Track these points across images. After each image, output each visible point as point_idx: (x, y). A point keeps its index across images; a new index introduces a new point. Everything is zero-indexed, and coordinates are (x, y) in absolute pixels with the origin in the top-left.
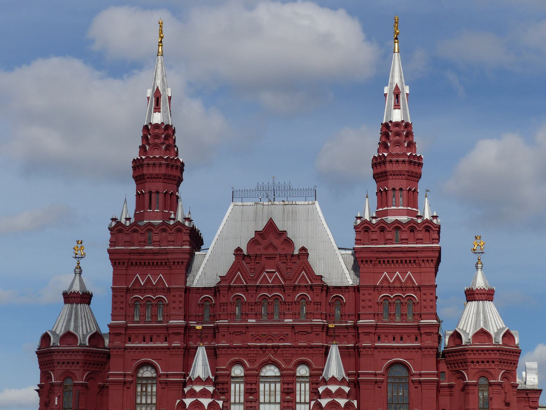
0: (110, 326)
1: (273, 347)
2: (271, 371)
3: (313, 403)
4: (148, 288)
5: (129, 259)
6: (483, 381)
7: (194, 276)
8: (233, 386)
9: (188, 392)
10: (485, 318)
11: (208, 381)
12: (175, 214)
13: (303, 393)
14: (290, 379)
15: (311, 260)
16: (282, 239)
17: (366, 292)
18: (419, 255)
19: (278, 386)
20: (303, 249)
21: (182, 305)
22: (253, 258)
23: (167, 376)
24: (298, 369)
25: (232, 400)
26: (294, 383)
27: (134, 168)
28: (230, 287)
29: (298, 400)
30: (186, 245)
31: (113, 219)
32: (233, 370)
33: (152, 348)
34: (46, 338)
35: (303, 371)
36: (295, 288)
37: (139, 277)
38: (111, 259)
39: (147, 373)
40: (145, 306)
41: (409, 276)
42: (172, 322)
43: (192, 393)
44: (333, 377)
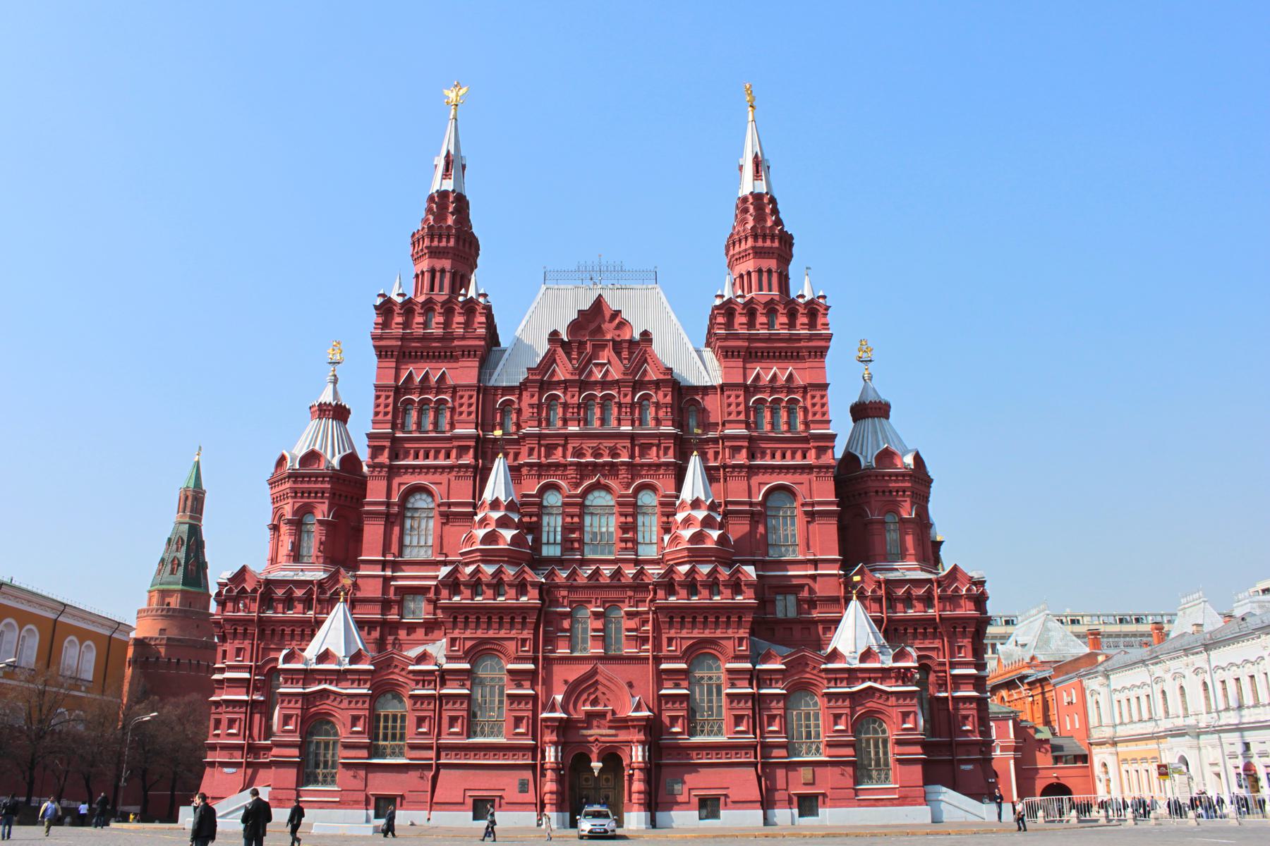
0: (370, 436)
1: (606, 464)
2: (599, 499)
3: (667, 538)
4: (424, 386)
5: (401, 347)
6: (888, 518)
7: (491, 375)
10: (886, 439)
11: (511, 506)
12: (467, 291)
14: (630, 510)
15: (656, 347)
16: (617, 321)
17: (733, 393)
18: (802, 344)
20: (646, 335)
21: (473, 408)
22: (575, 345)
23: (449, 505)
24: (640, 496)
25: (544, 540)
26: (634, 516)
31: (383, 295)
34: (282, 460)
35: (647, 499)
36: (637, 386)
38: (375, 347)
39: (420, 501)
40: (421, 412)
41: (791, 374)
42: (457, 431)
43: (484, 522)
44: (697, 499)
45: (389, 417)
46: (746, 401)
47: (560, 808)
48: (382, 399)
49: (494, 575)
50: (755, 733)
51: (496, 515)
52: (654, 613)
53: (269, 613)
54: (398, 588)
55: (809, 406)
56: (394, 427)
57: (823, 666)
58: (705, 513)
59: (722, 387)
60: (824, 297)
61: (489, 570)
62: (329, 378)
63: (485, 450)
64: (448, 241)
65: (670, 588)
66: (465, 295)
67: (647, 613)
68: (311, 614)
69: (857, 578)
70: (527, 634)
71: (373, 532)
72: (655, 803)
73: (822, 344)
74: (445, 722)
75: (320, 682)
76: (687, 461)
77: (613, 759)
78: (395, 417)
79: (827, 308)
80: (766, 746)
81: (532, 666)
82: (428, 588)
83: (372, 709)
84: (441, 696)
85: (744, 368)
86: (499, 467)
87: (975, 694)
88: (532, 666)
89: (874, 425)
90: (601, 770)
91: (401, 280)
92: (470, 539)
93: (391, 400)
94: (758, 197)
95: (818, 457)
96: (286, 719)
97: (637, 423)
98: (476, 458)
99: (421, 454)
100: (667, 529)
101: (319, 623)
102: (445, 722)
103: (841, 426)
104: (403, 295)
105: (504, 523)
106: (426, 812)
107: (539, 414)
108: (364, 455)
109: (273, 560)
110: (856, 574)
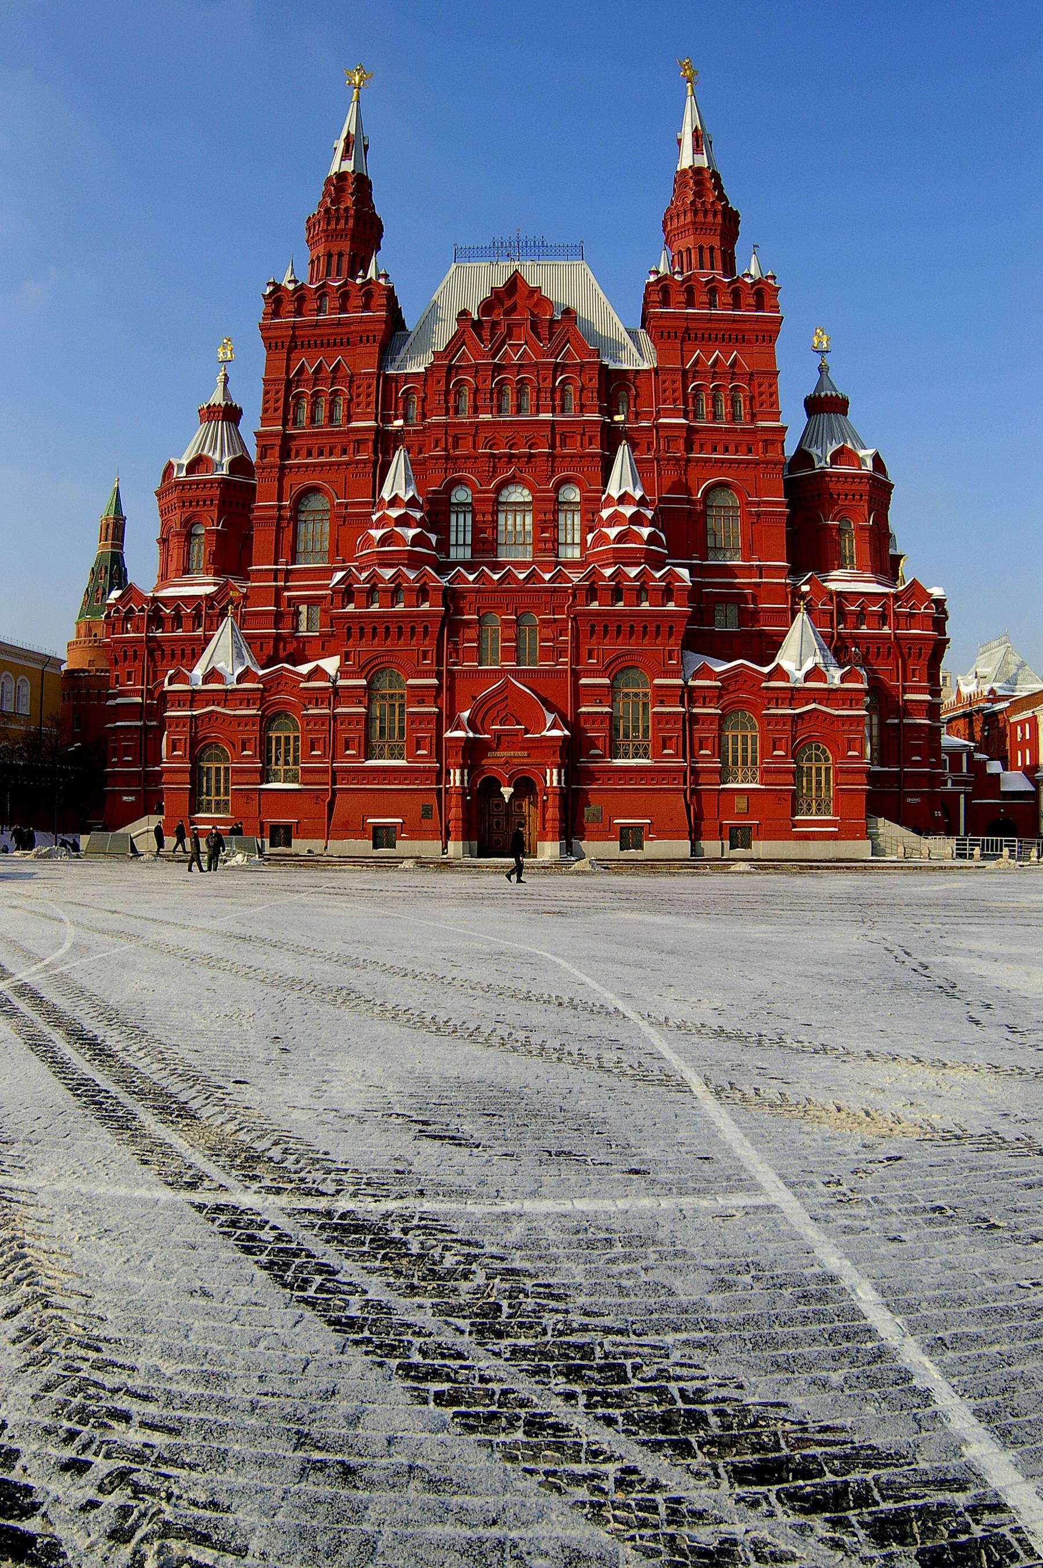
0: (258, 435)
1: (518, 456)
3: (590, 537)
8: (453, 517)
9: (379, 519)
11: (412, 503)
12: (366, 272)
13: (569, 527)
19: (529, 519)
20: (567, 311)
21: (373, 398)
25: (453, 541)
26: (556, 512)
27: (309, 229)
28: (450, 367)
29: (562, 540)
30: (381, 311)
31: (274, 284)
32: (453, 493)
33: (322, 465)
36: (558, 368)
37: (306, 364)
42: (354, 424)
45: (280, 413)
46: (685, 387)
47: (466, 837)
48: (271, 394)
49: (392, 580)
50: (684, 757)
51: (394, 513)
52: (574, 620)
53: (159, 634)
54: (290, 598)
55: (756, 395)
56: (284, 424)
57: (763, 685)
58: (634, 509)
59: (656, 370)
60: (774, 277)
61: (388, 573)
62: (220, 377)
63: (385, 443)
64: (346, 223)
65: (592, 593)
66: (364, 277)
67: (565, 621)
68: (199, 632)
69: (805, 588)
70: (429, 645)
71: (262, 539)
72: (571, 830)
73: (770, 327)
74: (341, 744)
75: (207, 705)
76: (614, 452)
77: (526, 787)
78: (286, 412)
79: (777, 289)
80: (695, 772)
81: (435, 681)
82: (324, 597)
83: (264, 730)
84: (335, 716)
85: (682, 350)
86: (399, 461)
87: (927, 722)
88: (435, 681)
89: (829, 419)
90: (512, 796)
91: (294, 267)
92: (368, 540)
93: (282, 394)
94: (697, 171)
95: (765, 451)
96: (173, 746)
97: (558, 409)
98: (375, 453)
99: (315, 451)
100: (588, 526)
101: (207, 640)
102: (341, 744)
103: (793, 419)
104: (295, 281)
105: (404, 521)
106: (321, 842)
107: (446, 401)
108: (254, 456)
109: (164, 578)
110: (804, 584)
